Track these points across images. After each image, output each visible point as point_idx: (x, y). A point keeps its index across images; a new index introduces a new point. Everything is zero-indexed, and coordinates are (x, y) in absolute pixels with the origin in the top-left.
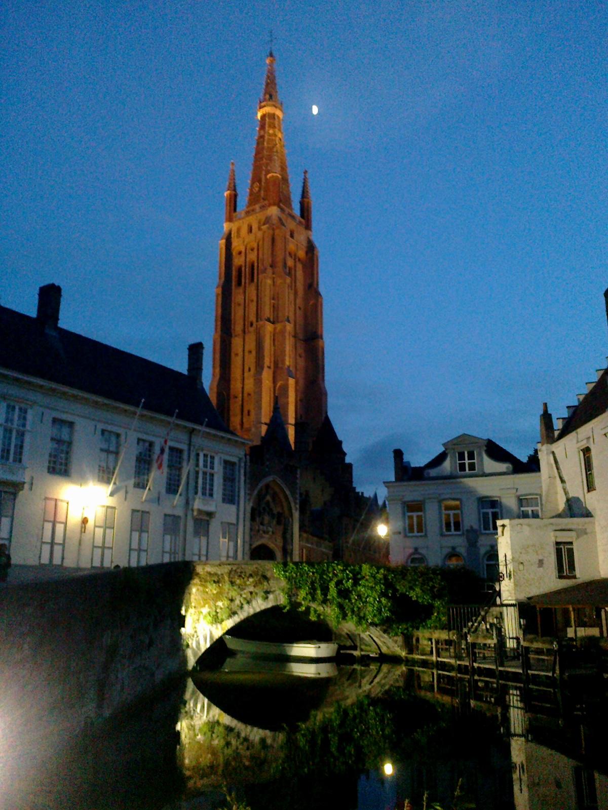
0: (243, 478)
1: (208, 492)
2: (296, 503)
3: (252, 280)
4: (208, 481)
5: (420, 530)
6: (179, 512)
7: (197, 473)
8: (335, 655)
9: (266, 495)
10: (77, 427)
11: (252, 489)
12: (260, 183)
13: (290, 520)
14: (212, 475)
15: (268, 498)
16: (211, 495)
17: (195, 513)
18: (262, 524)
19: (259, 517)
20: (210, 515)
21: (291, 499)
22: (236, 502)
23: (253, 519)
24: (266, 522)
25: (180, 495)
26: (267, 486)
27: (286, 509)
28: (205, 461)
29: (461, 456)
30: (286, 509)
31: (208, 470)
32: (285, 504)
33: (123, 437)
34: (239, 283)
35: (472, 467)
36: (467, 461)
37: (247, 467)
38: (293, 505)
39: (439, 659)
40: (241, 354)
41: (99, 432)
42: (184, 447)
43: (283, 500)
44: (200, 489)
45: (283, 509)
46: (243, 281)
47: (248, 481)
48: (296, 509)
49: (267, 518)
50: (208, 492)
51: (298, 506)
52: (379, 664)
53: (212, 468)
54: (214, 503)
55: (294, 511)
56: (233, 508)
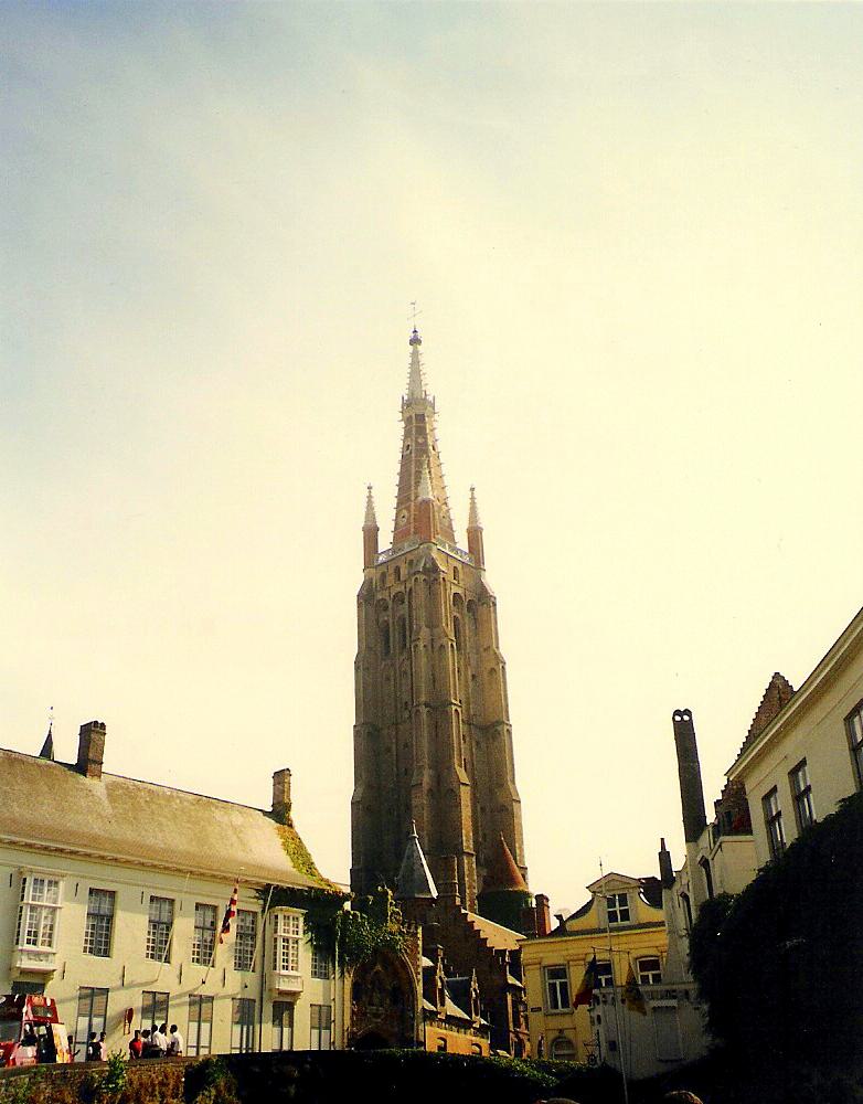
7: (276, 939)
10: (119, 898)
12: (409, 511)
15: (379, 967)
20: (295, 994)
24: (376, 1001)
29: (611, 903)
33: (177, 905)
35: (625, 914)
36: (618, 908)
41: (147, 899)
42: (259, 910)
44: (280, 963)
49: (377, 997)
50: (291, 965)
51: (420, 977)
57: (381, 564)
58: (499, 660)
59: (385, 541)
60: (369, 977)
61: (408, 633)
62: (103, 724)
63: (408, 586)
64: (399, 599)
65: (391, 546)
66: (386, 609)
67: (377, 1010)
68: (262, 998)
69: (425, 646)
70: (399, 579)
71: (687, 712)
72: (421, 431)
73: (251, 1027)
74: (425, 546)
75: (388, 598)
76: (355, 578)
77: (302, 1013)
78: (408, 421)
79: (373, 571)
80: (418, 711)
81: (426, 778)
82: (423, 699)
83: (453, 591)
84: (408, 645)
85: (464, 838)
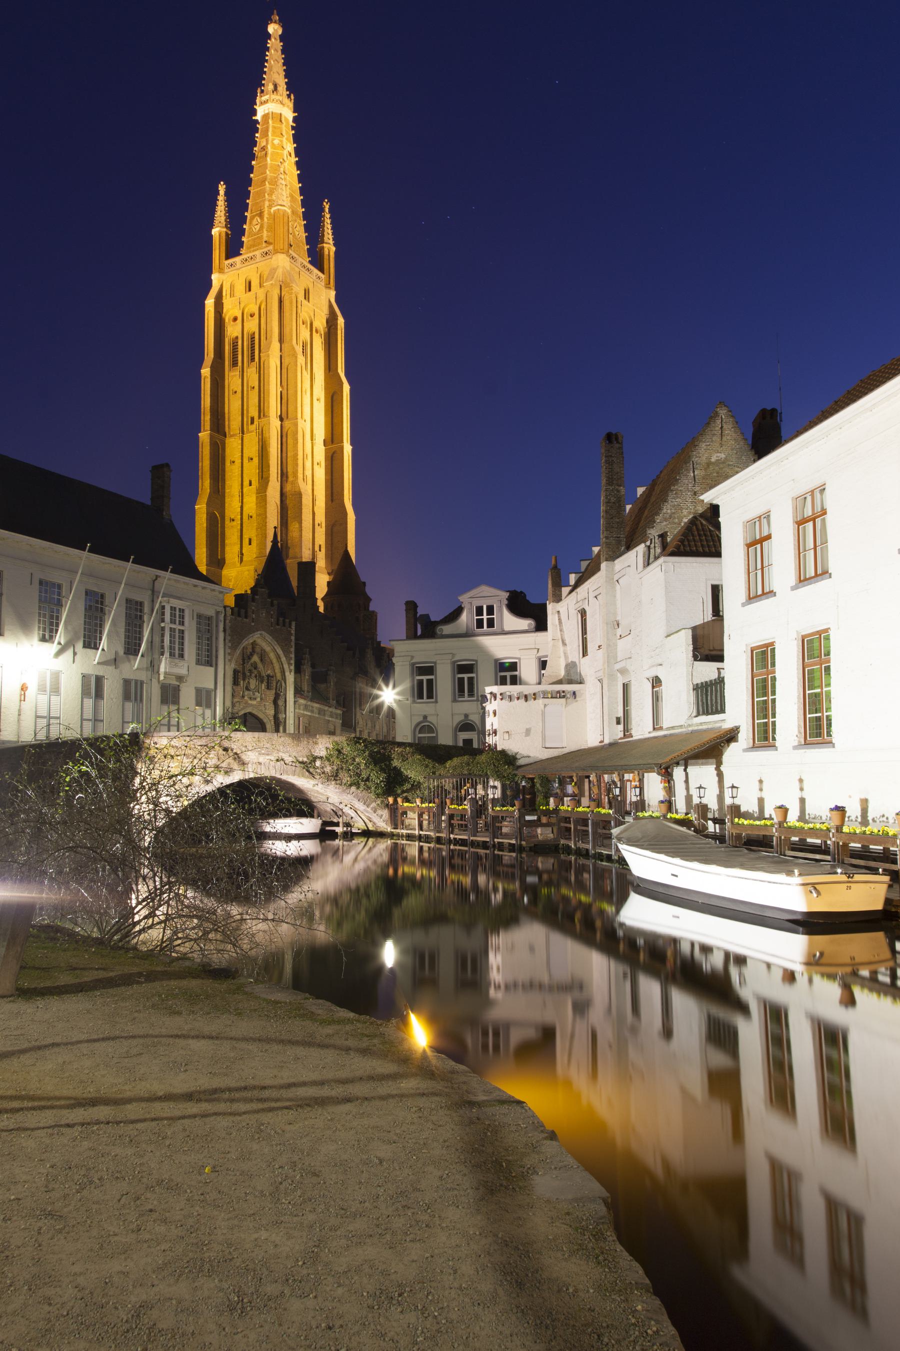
0: (221, 635)
1: (177, 652)
2: (289, 664)
3: (253, 359)
5: (430, 696)
6: (143, 676)
7: (163, 629)
8: (318, 831)
9: (251, 655)
11: (234, 647)
13: (283, 684)
14: (182, 632)
16: (182, 656)
17: (162, 678)
18: (247, 689)
19: (244, 680)
20: (180, 678)
23: (235, 682)
24: (252, 686)
25: (142, 656)
26: (254, 644)
27: (278, 671)
28: (173, 615)
29: (479, 611)
30: (278, 671)
31: (177, 627)
34: (234, 363)
35: (491, 623)
37: (227, 621)
38: (286, 666)
39: (421, 833)
40: (238, 462)
43: (275, 661)
47: (228, 638)
49: (253, 683)
51: (292, 667)
52: (366, 839)
55: (287, 674)
60: (248, 666)
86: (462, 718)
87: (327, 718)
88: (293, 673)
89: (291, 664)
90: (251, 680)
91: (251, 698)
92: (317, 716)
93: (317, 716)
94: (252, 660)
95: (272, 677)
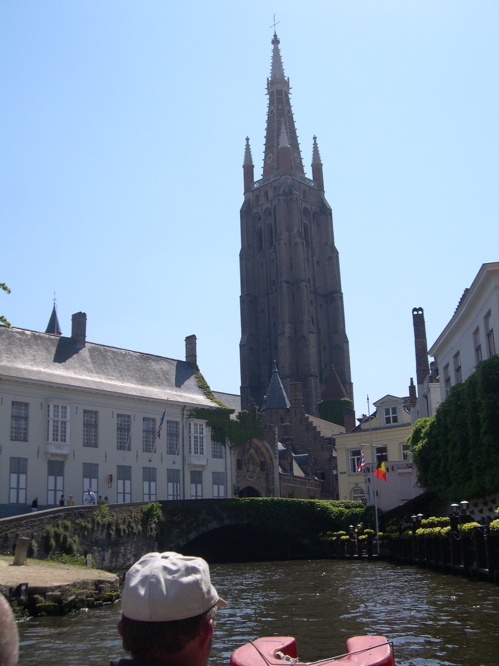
2: (275, 454)
4: (199, 443)
6: (178, 466)
7: (190, 437)
9: (249, 449)
13: (272, 467)
15: (252, 451)
18: (248, 471)
20: (203, 466)
21: (271, 451)
22: (224, 458)
24: (251, 469)
28: (196, 428)
32: (267, 455)
35: (395, 420)
36: (391, 415)
41: (115, 416)
44: (193, 450)
45: (265, 458)
46: (263, 244)
48: (276, 458)
49: (251, 467)
50: (199, 451)
51: (277, 456)
53: (201, 433)
54: (205, 460)
55: (274, 460)
56: (221, 461)
57: (255, 190)
58: (335, 252)
59: (258, 175)
61: (274, 235)
62: (84, 313)
63: (274, 203)
64: (268, 212)
65: (262, 177)
66: (260, 219)
67: (252, 474)
68: (184, 469)
69: (285, 244)
70: (268, 199)
71: (421, 309)
72: (280, 101)
73: (178, 484)
74: (284, 177)
75: (260, 212)
76: (240, 200)
77: (207, 478)
78: (271, 94)
79: (251, 194)
80: (281, 286)
81: (288, 330)
82: (284, 278)
83: (303, 206)
84: (274, 243)
85: (312, 366)
86: (354, 485)
87: (307, 487)
88: (277, 459)
89: (276, 454)
90: (250, 466)
91: (250, 477)
92: (299, 486)
93: (299, 486)
94: (250, 453)
95: (264, 462)
